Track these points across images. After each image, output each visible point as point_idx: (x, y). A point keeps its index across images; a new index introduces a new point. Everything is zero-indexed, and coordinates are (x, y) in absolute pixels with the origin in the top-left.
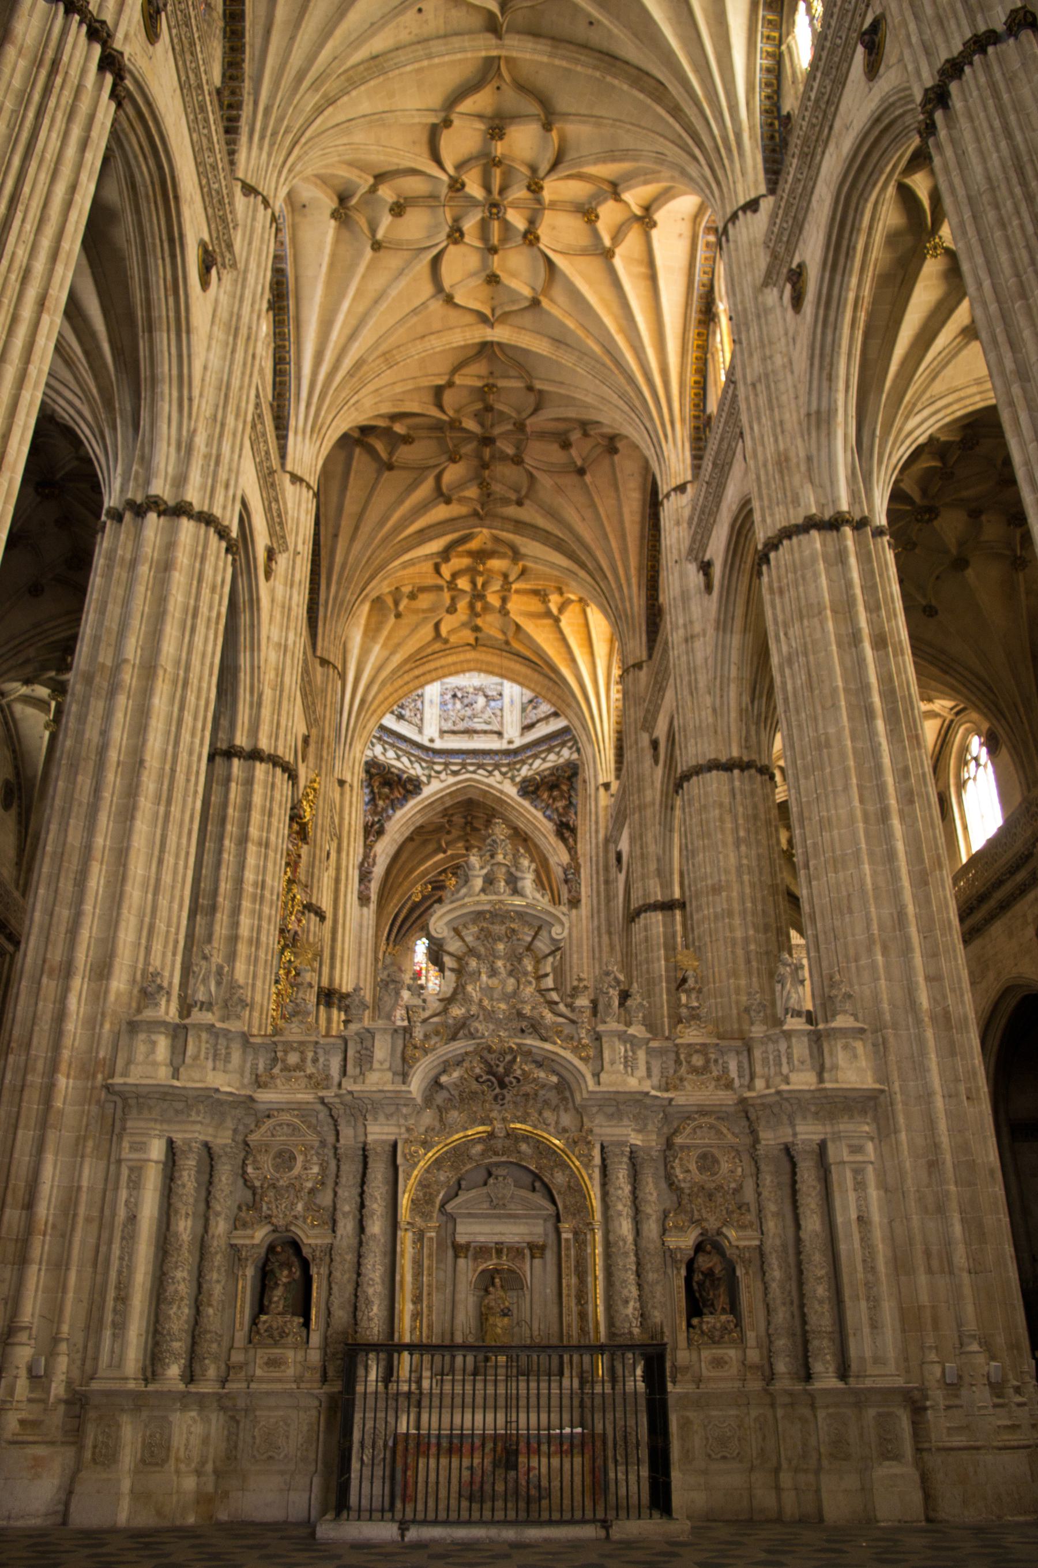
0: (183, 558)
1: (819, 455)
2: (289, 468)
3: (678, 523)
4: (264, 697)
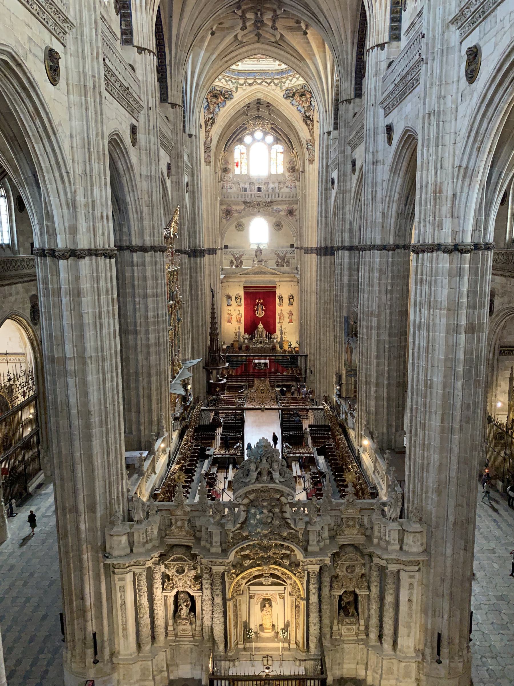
0: (85, 285)
1: (461, 195)
3: (376, 75)
4: (144, 214)
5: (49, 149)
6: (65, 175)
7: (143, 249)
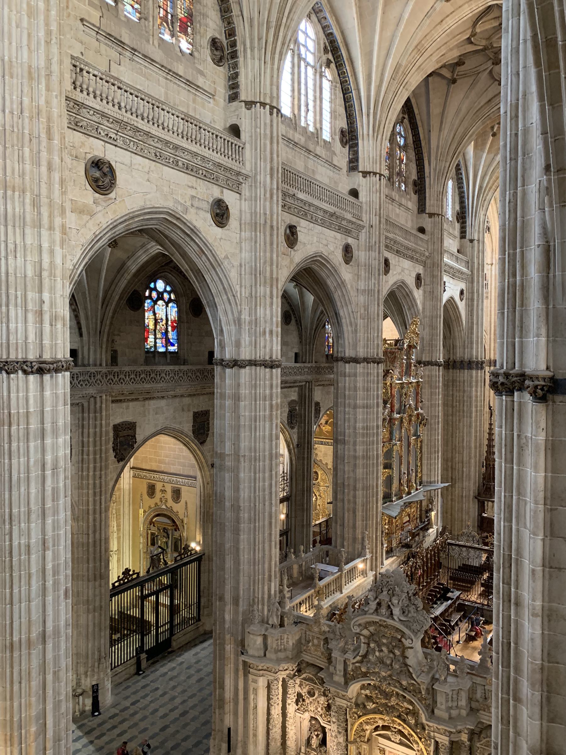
0: (244, 391)
2: (360, 169)
5: (216, 278)
6: (231, 298)
7: (355, 360)
